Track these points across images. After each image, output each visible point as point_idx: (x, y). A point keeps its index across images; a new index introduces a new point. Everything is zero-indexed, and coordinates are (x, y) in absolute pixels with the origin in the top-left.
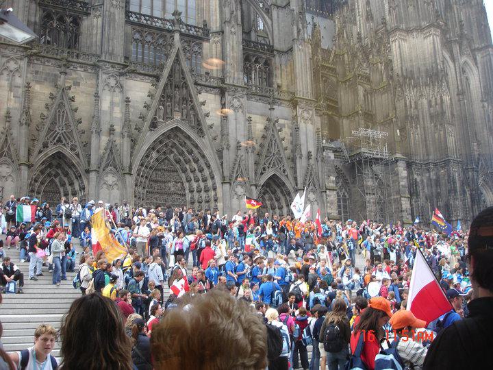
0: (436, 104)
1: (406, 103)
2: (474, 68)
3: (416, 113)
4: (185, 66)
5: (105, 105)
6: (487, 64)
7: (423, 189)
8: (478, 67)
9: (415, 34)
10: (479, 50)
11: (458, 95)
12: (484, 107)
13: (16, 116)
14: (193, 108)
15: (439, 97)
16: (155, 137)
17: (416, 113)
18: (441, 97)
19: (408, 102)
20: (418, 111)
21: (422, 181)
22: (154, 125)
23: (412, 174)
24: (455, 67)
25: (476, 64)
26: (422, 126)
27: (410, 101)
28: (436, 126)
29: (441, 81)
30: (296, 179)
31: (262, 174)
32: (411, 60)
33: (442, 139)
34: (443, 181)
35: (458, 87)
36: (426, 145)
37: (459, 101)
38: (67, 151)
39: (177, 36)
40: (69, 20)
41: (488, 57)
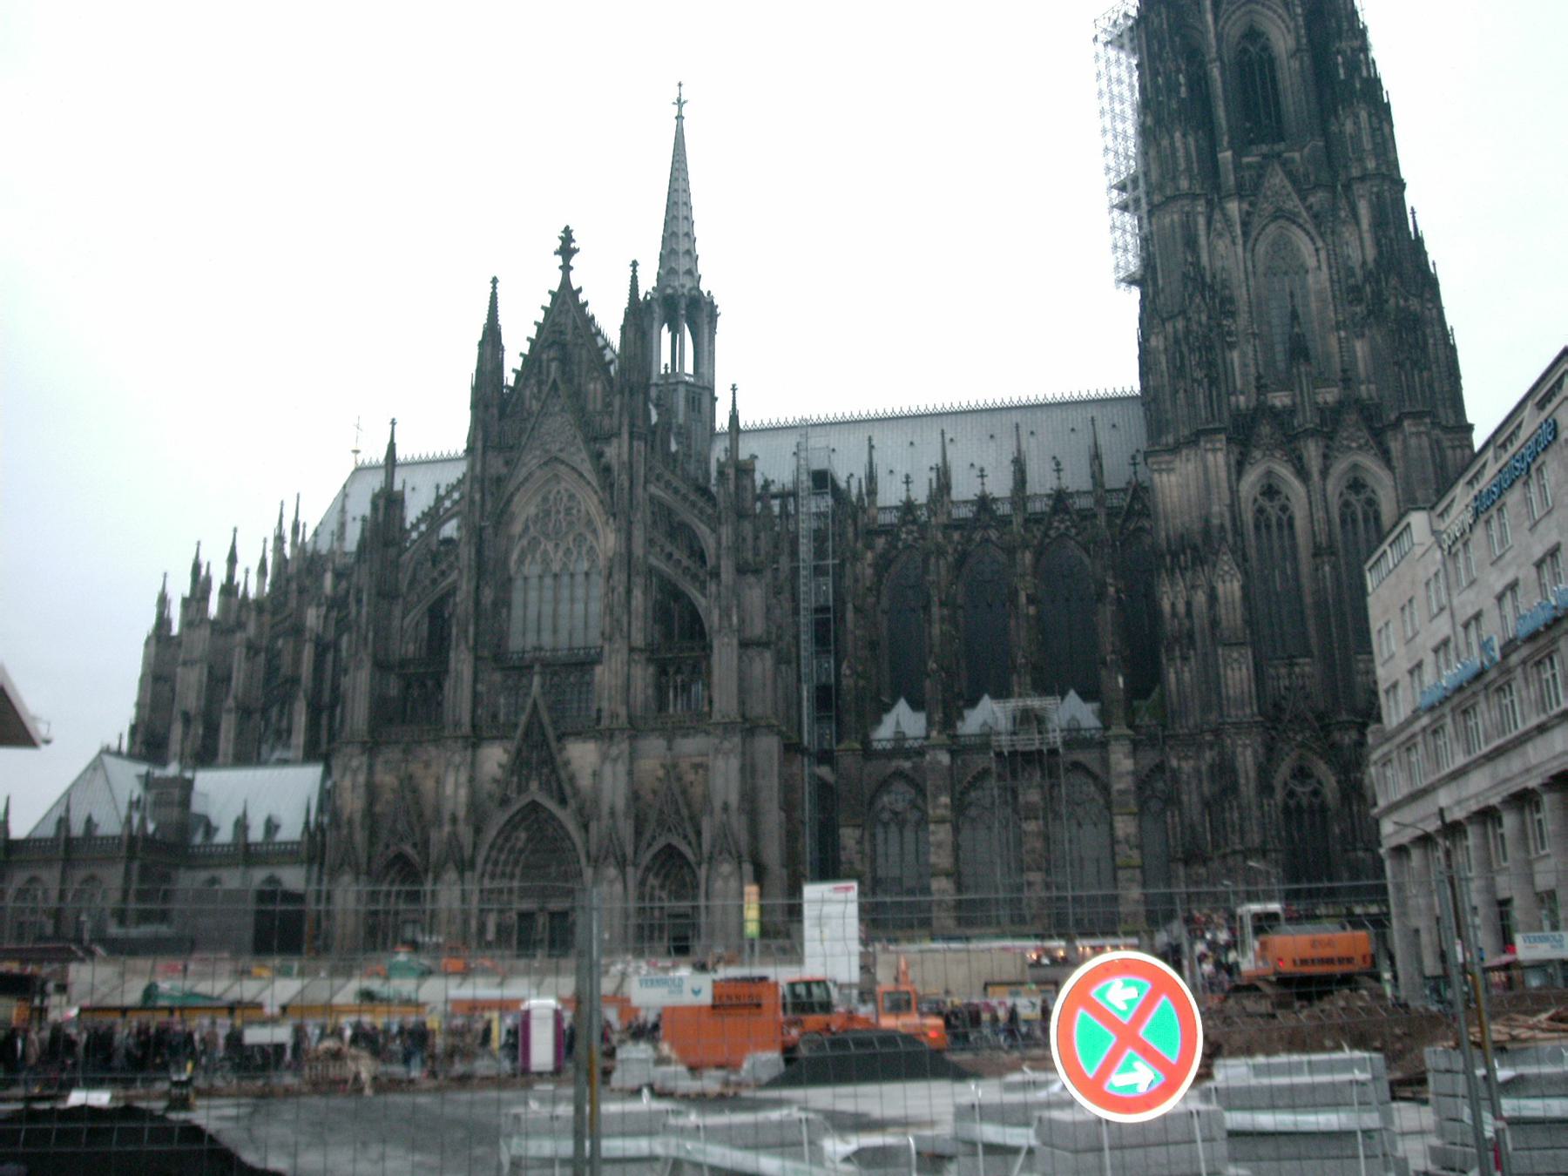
4: (546, 718)
5: (449, 790)
8: (1390, 468)
9: (1184, 452)
11: (1315, 555)
13: (358, 817)
14: (554, 771)
16: (506, 817)
17: (1186, 622)
19: (1166, 606)
22: (504, 802)
30: (700, 846)
31: (650, 845)
38: (408, 849)
39: (537, 680)
40: (430, 683)
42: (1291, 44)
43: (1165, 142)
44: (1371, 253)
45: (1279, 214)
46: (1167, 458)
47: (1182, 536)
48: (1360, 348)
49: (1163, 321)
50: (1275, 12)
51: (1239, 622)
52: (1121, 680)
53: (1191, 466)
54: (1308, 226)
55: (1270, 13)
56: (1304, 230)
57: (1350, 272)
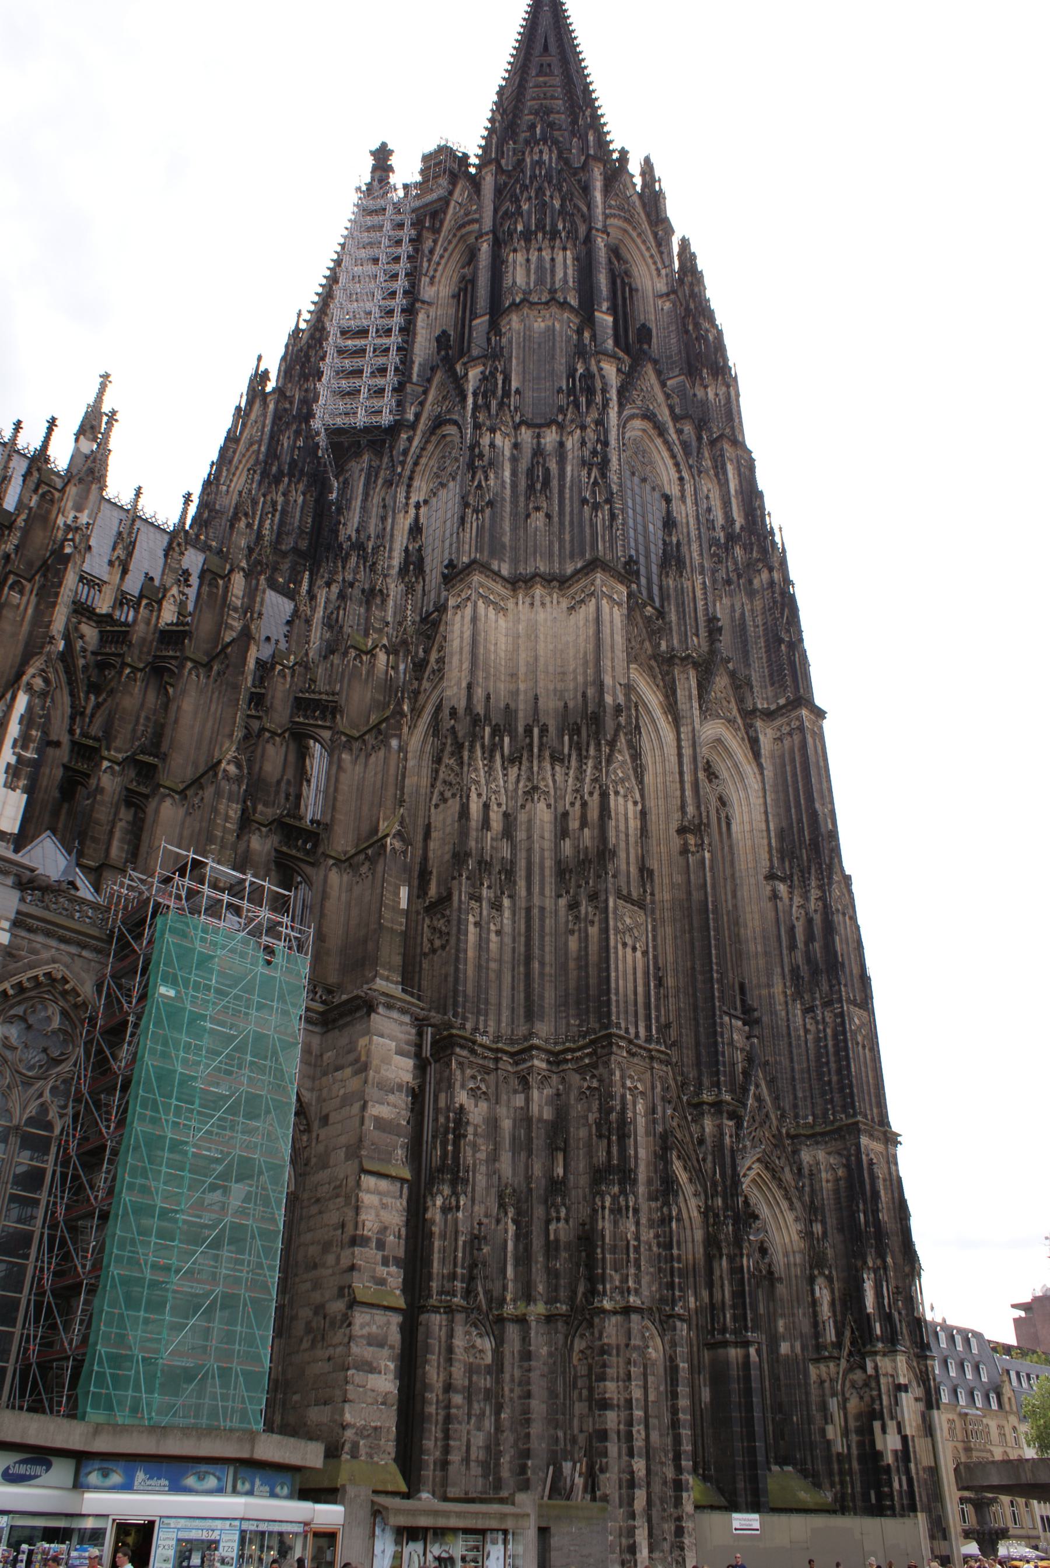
0: (584, 823)
1: (464, 813)
2: (749, 769)
3: (506, 853)
6: (793, 760)
7: (494, 1157)
8: (760, 766)
9: (538, 591)
10: (769, 715)
11: (682, 831)
12: (775, 896)
15: (594, 802)
17: (506, 853)
18: (604, 796)
20: (514, 847)
21: (493, 1123)
23: (450, 1086)
24: (679, 740)
25: (757, 755)
26: (523, 904)
27: (486, 806)
28: (574, 906)
29: (612, 744)
32: (514, 676)
33: (593, 958)
34: (583, 1133)
35: (683, 808)
36: (528, 975)
37: (685, 851)
41: (796, 738)
42: (661, 286)
43: (546, 255)
44: (739, 520)
45: (649, 416)
46: (499, 588)
47: (509, 712)
48: (721, 610)
49: (517, 427)
50: (648, 249)
51: (633, 869)
52: (404, 892)
53: (541, 615)
54: (676, 450)
55: (643, 248)
56: (670, 450)
57: (711, 525)
